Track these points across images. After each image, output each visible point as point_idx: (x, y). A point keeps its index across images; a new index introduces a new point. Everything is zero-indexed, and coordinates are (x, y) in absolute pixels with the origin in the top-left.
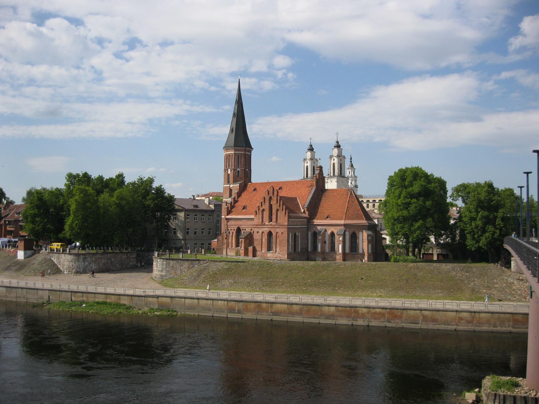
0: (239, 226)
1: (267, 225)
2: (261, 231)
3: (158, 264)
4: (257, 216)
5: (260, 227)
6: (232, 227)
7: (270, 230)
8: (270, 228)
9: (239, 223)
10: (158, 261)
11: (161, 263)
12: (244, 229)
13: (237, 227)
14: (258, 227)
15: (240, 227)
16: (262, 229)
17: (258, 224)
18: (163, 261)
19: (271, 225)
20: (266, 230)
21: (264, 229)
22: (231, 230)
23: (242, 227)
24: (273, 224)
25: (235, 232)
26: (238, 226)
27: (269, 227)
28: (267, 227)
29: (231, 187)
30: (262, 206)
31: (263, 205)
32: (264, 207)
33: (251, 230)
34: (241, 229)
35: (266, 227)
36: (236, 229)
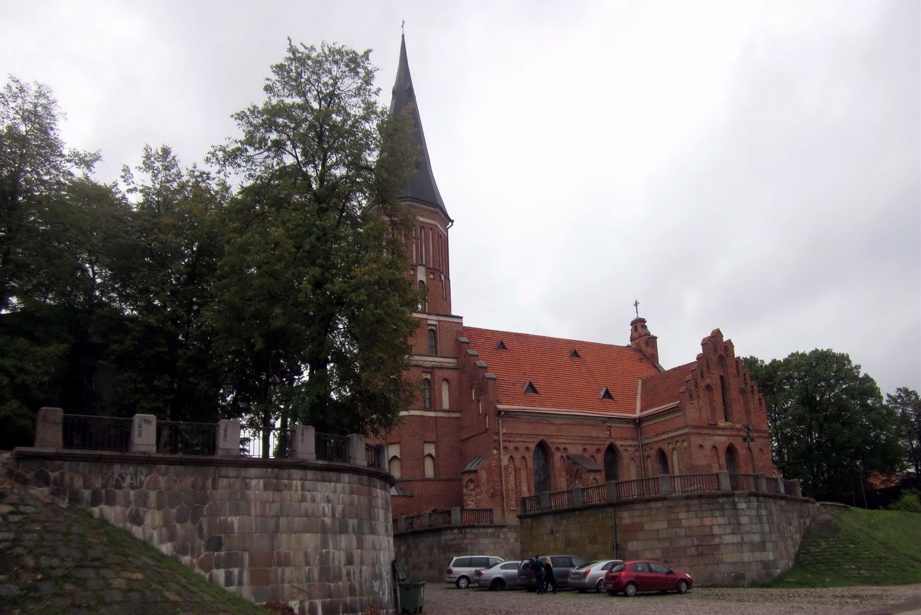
0: (544, 438)
1: (724, 429)
2: (708, 444)
3: (744, 520)
4: (695, 401)
5: (706, 431)
6: (517, 439)
7: (731, 441)
8: (731, 435)
9: (545, 431)
10: (742, 506)
11: (754, 513)
12: (562, 447)
13: (537, 441)
14: (699, 431)
15: (549, 441)
16: (711, 438)
17: (698, 424)
18: (758, 508)
19: (731, 429)
20: (722, 441)
21: (716, 438)
22: (516, 448)
23: (554, 440)
24: (738, 426)
25: (530, 456)
26: (540, 438)
27: (729, 433)
28: (723, 433)
29: (430, 322)
30: (702, 377)
31: (706, 375)
32: (708, 381)
33: (585, 450)
34: (553, 447)
35: (719, 432)
36: (533, 446)
